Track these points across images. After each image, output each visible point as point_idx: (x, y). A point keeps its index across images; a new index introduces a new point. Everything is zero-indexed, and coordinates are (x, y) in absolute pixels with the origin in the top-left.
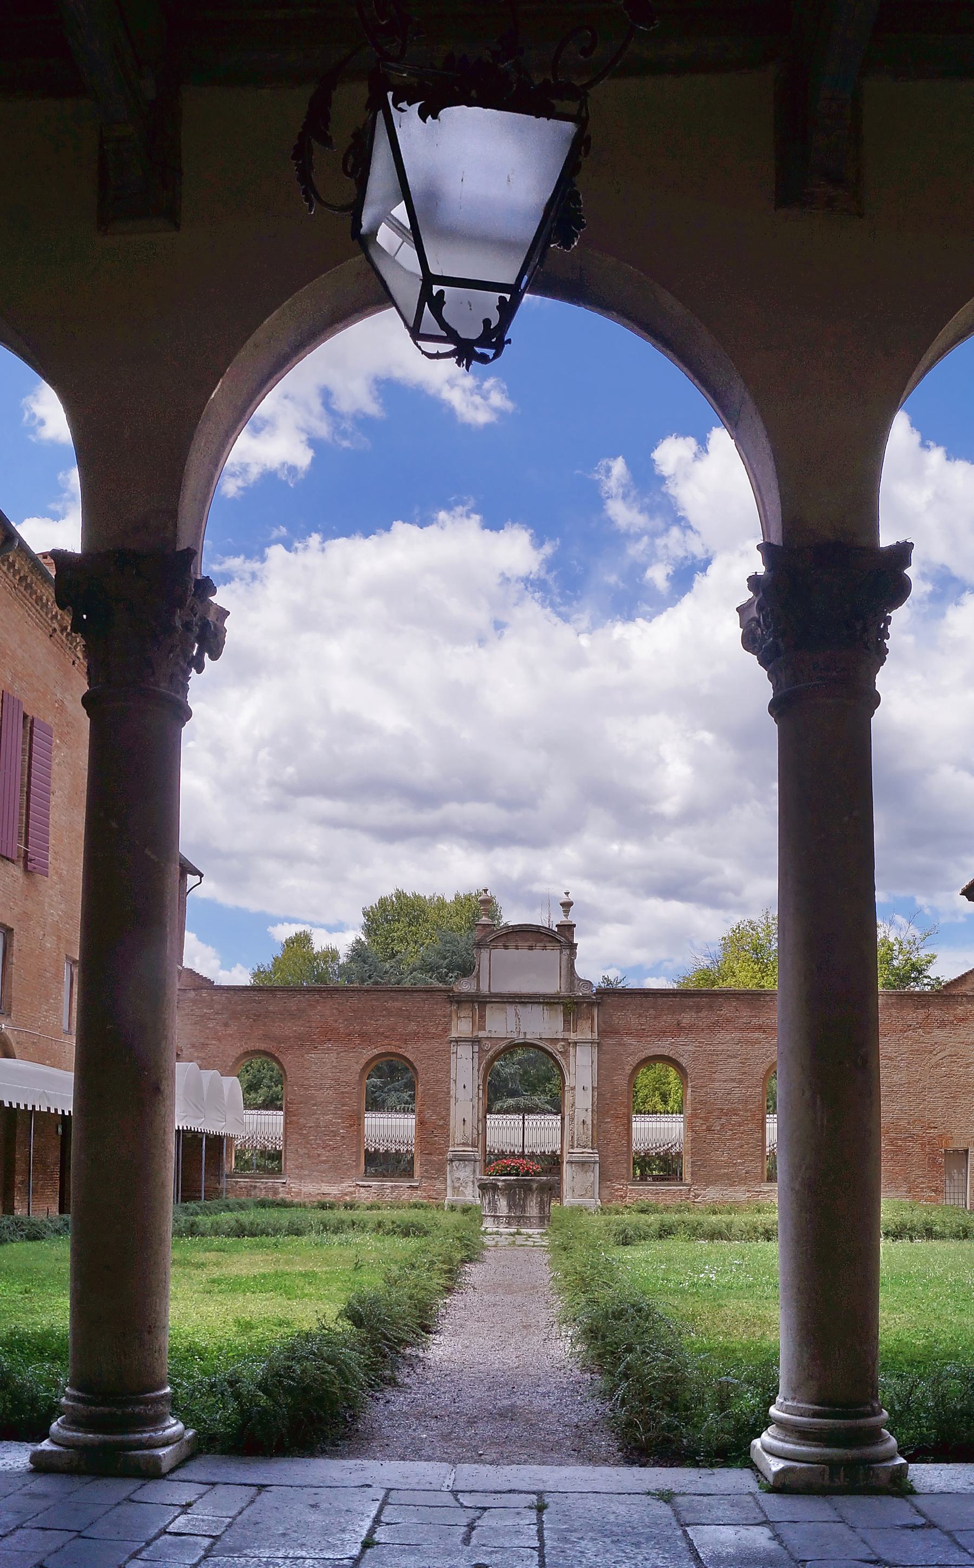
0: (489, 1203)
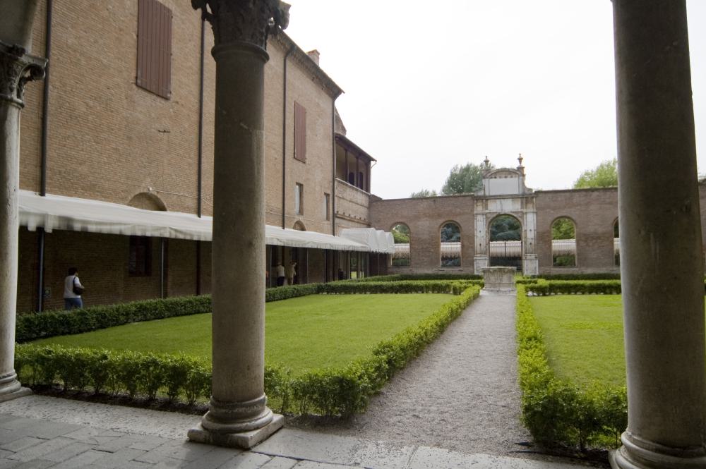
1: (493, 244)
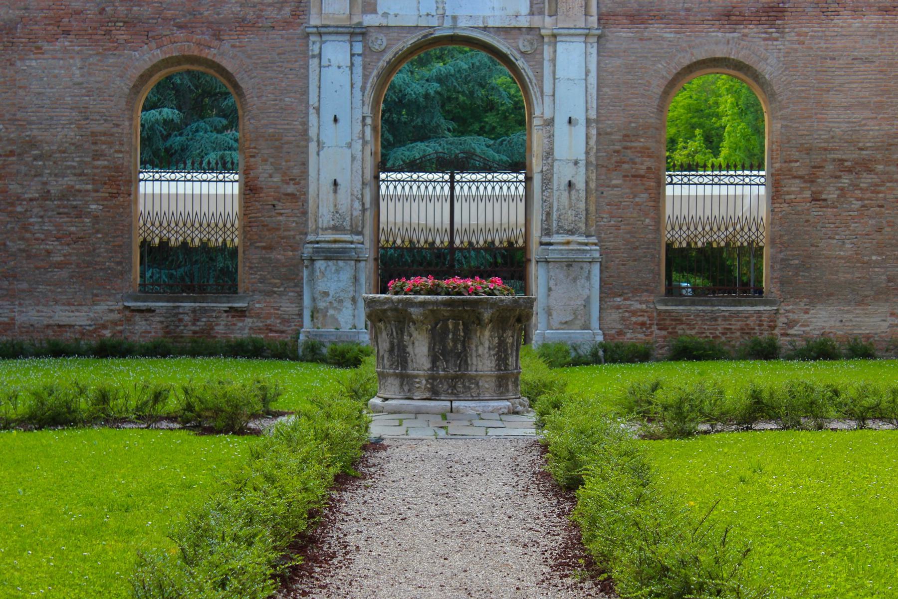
0: (391, 351)
1: (394, 183)
